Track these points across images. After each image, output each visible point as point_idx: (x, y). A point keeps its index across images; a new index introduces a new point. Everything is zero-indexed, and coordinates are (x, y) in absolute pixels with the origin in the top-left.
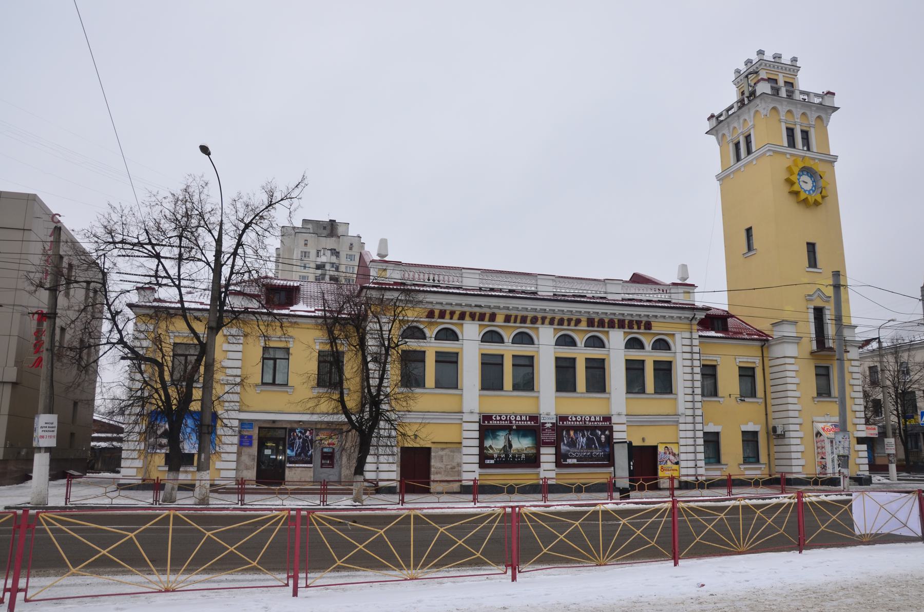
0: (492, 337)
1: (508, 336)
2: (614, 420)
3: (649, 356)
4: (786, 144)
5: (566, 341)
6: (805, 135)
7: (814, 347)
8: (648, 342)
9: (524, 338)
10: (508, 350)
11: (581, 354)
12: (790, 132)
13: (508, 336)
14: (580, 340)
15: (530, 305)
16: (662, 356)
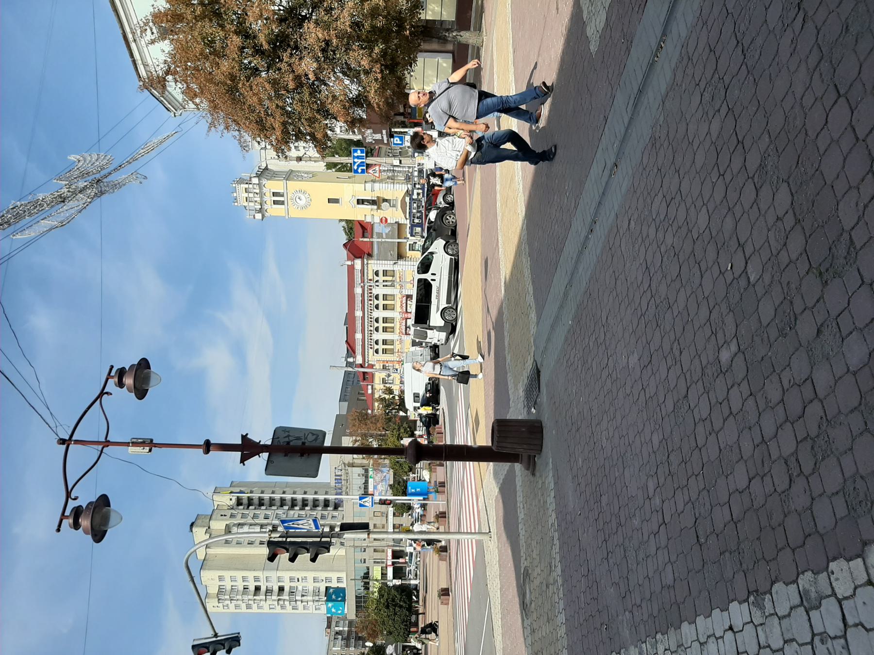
0: (377, 329)
1: (376, 325)
2: (404, 293)
3: (381, 278)
4: (283, 206)
5: (377, 307)
6: (274, 194)
7: (375, 207)
8: (376, 278)
9: (377, 320)
10: (381, 325)
11: (381, 302)
12: (275, 202)
13: (376, 325)
14: (376, 302)
15: (366, 321)
16: (381, 274)
